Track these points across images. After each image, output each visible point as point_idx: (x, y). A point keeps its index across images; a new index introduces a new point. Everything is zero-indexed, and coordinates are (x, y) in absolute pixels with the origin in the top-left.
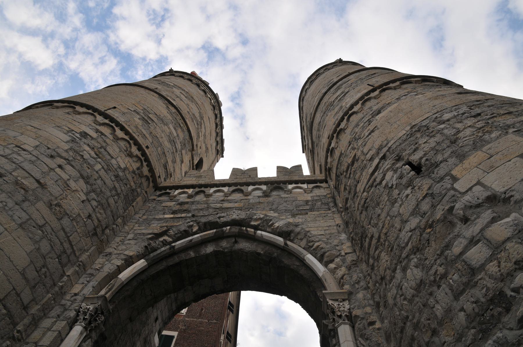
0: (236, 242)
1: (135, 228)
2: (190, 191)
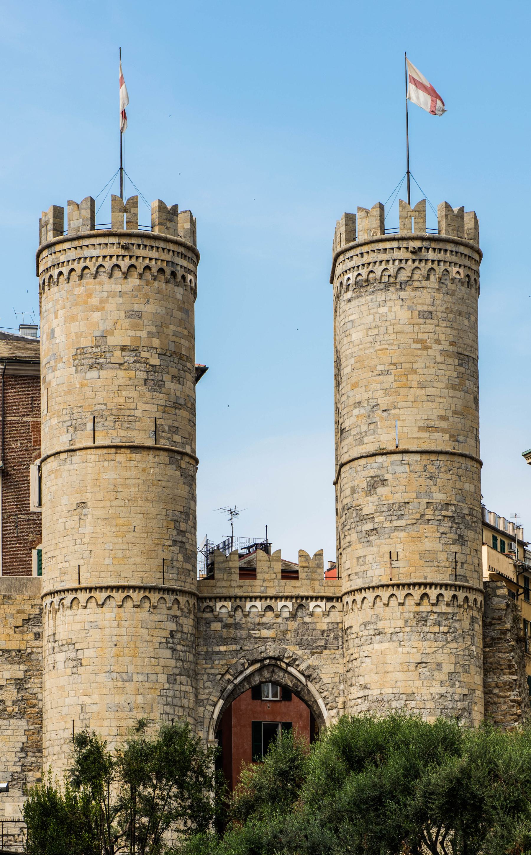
0: (273, 671)
1: (205, 666)
2: (228, 604)
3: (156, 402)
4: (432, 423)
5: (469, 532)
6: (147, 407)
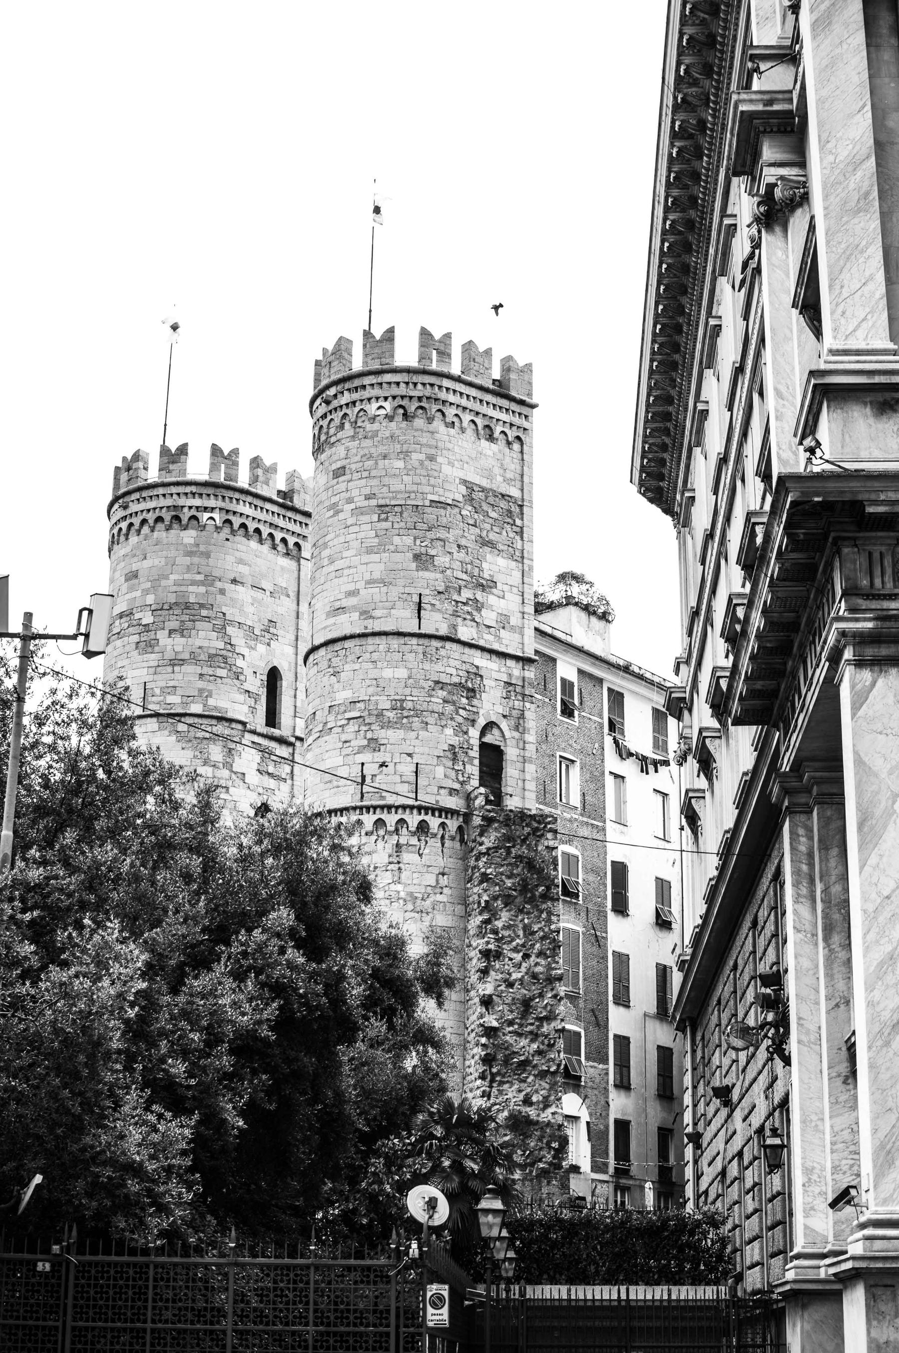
3: (145, 664)
4: (337, 605)
5: (390, 733)
6: (136, 673)
